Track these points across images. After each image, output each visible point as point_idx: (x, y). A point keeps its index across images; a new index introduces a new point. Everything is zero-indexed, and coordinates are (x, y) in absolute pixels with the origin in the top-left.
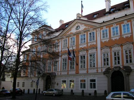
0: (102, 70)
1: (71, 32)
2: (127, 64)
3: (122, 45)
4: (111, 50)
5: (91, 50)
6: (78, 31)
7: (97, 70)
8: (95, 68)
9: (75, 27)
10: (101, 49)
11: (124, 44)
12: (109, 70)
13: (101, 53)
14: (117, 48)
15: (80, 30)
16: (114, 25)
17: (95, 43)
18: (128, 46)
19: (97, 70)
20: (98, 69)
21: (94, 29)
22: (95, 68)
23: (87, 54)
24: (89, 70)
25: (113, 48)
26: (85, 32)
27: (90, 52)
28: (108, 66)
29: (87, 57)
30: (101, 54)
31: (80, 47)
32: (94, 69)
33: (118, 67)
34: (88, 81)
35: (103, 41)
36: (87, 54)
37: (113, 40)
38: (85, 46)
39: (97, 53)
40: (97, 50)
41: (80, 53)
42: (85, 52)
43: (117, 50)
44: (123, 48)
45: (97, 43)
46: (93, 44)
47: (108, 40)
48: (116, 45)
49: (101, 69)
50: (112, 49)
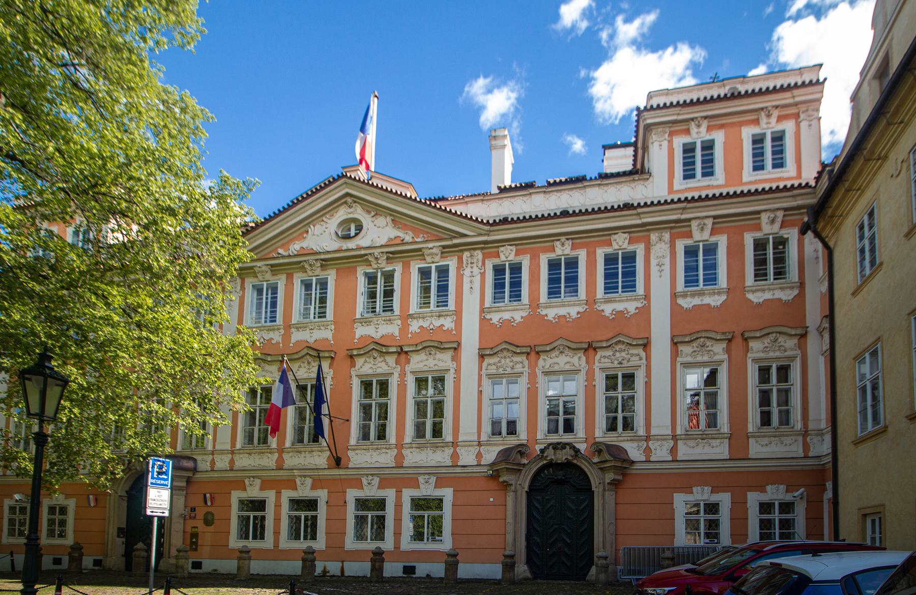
1: (305, 244)
2: (612, 434)
3: (594, 345)
4: (533, 367)
5: (422, 356)
6: (351, 244)
7: (455, 456)
9: (333, 223)
10: (482, 357)
11: (607, 340)
13: (480, 376)
14: (568, 359)
15: (363, 241)
16: (558, 243)
17: (448, 323)
18: (623, 354)
21: (446, 251)
23: (403, 375)
25: (543, 356)
26: (392, 257)
27: (420, 363)
28: (512, 441)
31: (361, 331)
35: (495, 318)
36: (403, 375)
37: (550, 317)
38: (393, 329)
40: (456, 358)
41: (359, 362)
42: (391, 360)
43: (568, 367)
44: (597, 364)
45: (458, 323)
46: (437, 323)
47: (525, 314)
50: (541, 363)
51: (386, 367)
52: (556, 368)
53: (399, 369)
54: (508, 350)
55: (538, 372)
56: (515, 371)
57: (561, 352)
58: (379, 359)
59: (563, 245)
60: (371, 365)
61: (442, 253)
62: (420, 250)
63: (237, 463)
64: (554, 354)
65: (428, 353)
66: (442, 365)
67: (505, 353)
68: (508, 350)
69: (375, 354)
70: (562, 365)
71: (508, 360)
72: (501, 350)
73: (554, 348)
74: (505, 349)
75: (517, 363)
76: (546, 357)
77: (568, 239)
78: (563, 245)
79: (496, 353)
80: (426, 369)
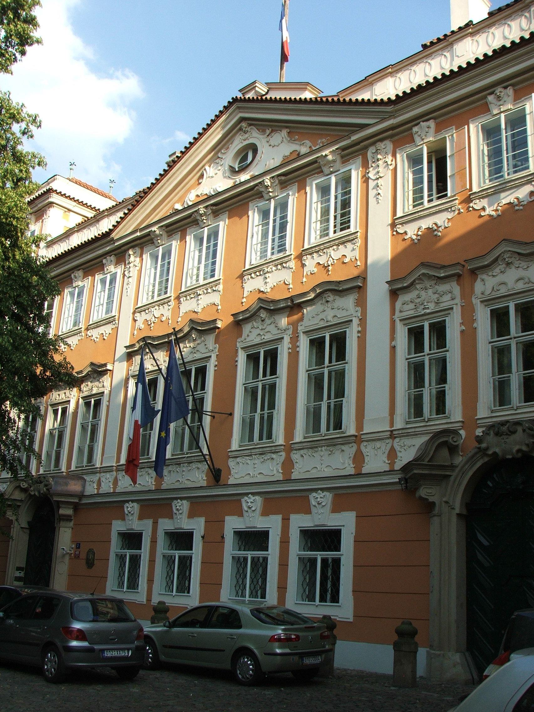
0: (392, 454)
4: (467, 295)
8: (347, 440)
10: (394, 294)
12: (445, 452)
14: (521, 273)
16: (491, 98)
19: (359, 458)
20: (367, 449)
22: (347, 440)
23: (295, 339)
24: (295, 456)
29: (294, 356)
30: (393, 337)
32: (332, 444)
33: (518, 423)
34: (285, 542)
39: (363, 321)
40: (362, 303)
41: (246, 328)
43: (520, 286)
48: (504, 248)
49: (385, 447)
50: (479, 287)
51: (275, 331)
52: (503, 291)
53: (290, 332)
54: (430, 277)
55: (476, 302)
56: (443, 306)
57: (508, 264)
58: (268, 321)
59: (499, 98)
60: (258, 331)
61: (342, 157)
62: (315, 162)
63: (119, 483)
64: (497, 270)
65: (324, 300)
66: (342, 315)
67: (428, 283)
68: (430, 277)
69: (263, 314)
70: (511, 284)
71: (430, 292)
72: (419, 278)
73: (496, 260)
74: (423, 274)
75: (444, 293)
76: (484, 277)
77: (505, 88)
78: (499, 98)
79: (412, 284)
80: (323, 324)
